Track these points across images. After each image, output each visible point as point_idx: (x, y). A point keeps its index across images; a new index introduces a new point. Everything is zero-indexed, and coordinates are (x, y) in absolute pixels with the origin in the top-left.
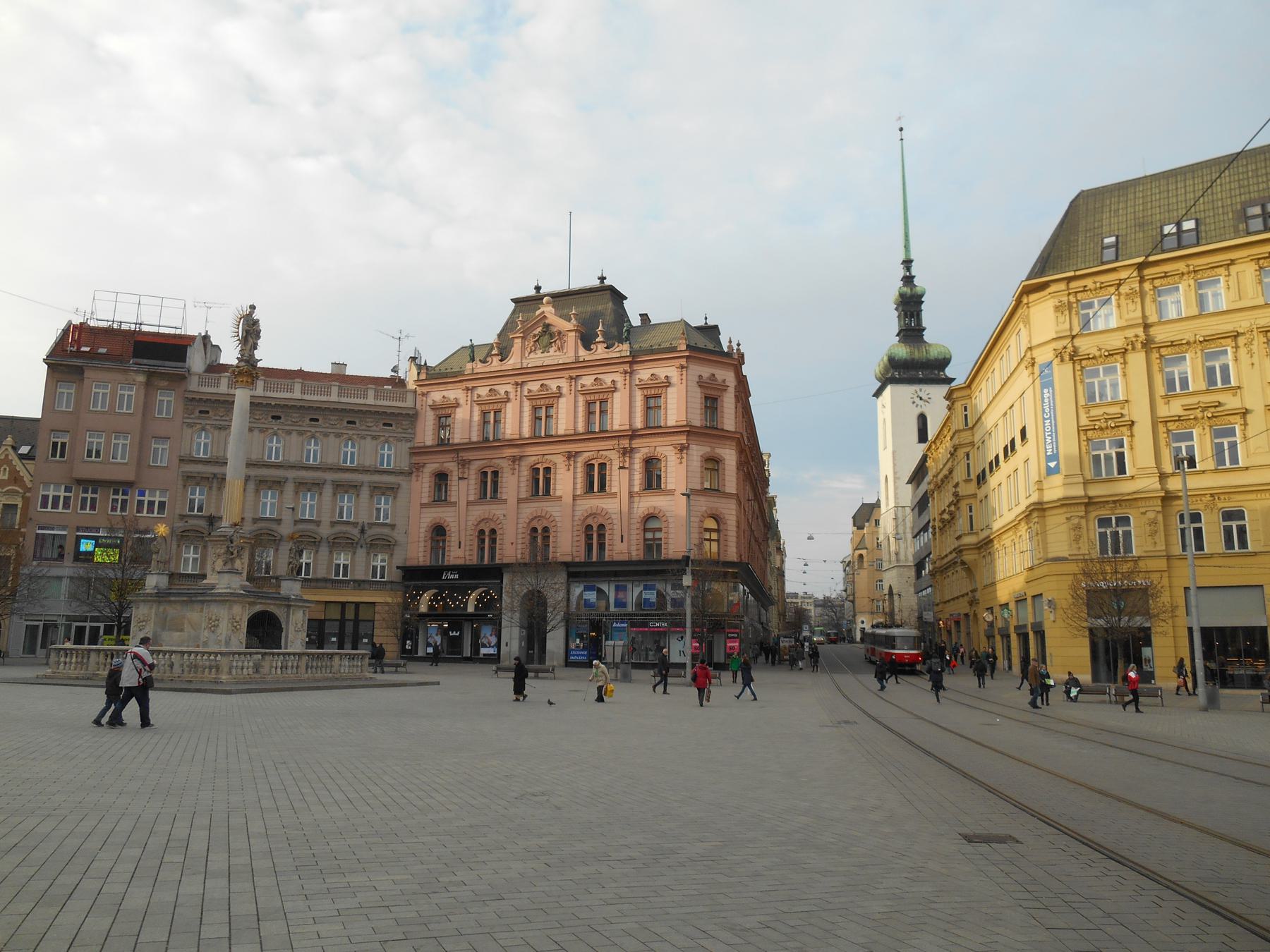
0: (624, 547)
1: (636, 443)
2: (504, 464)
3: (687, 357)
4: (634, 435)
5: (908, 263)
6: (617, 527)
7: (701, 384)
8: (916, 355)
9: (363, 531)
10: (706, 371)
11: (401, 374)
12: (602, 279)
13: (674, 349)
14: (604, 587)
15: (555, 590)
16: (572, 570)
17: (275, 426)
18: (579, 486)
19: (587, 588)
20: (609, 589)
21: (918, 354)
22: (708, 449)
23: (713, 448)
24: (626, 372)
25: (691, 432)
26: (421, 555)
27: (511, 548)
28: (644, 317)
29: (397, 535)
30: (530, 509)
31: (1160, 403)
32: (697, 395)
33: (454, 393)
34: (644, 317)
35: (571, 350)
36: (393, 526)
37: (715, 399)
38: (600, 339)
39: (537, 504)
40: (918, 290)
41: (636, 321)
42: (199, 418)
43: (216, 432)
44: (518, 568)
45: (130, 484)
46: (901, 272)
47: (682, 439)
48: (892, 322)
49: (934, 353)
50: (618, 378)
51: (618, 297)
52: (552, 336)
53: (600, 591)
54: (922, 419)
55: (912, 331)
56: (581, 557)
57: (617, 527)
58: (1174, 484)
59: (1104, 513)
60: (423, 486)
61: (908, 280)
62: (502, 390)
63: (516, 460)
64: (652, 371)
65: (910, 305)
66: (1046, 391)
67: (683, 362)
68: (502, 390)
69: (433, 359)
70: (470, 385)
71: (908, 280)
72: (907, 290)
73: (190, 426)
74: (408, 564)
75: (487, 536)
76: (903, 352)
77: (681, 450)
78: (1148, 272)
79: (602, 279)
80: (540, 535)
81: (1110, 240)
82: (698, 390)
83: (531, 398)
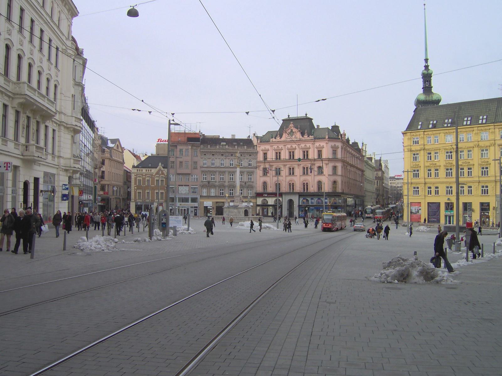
0: (313, 188)
1: (315, 162)
2: (282, 166)
3: (328, 141)
4: (315, 160)
5: (426, 60)
6: (311, 182)
7: (332, 147)
8: (428, 99)
9: (245, 184)
10: (333, 144)
11: (251, 138)
12: (306, 114)
13: (325, 138)
14: (307, 198)
15: (295, 199)
16: (300, 194)
17: (222, 157)
18: (301, 173)
19: (304, 199)
20: (309, 199)
21: (429, 98)
22: (334, 164)
23: (335, 164)
24: (312, 144)
25: (329, 160)
26: (261, 189)
27: (284, 188)
28: (318, 126)
29: (254, 184)
30: (289, 178)
31: (426, 163)
33: (267, 147)
34: (318, 126)
35: (298, 135)
36: (253, 182)
37: (336, 151)
38: (306, 134)
39: (291, 177)
40: (430, 72)
41: (316, 127)
42: (204, 156)
43: (208, 160)
44: (286, 193)
45: (189, 174)
46: (424, 64)
47: (327, 162)
48: (420, 83)
49: (435, 98)
50: (311, 145)
51: (310, 120)
52: (293, 133)
53: (307, 199)
55: (427, 89)
56: (302, 191)
57: (311, 182)
58: (427, 181)
59: (415, 186)
60: (260, 172)
61: (427, 67)
62: (280, 147)
63: (285, 166)
64: (320, 144)
65: (427, 77)
67: (327, 142)
68: (280, 147)
69: (260, 134)
70: (272, 145)
71: (427, 67)
72: (426, 72)
73: (202, 158)
74: (257, 192)
75: (278, 185)
76: (423, 98)
77: (327, 165)
78: (425, 133)
79: (306, 114)
80: (292, 185)
81: (420, 123)
82: (331, 149)
83: (288, 149)
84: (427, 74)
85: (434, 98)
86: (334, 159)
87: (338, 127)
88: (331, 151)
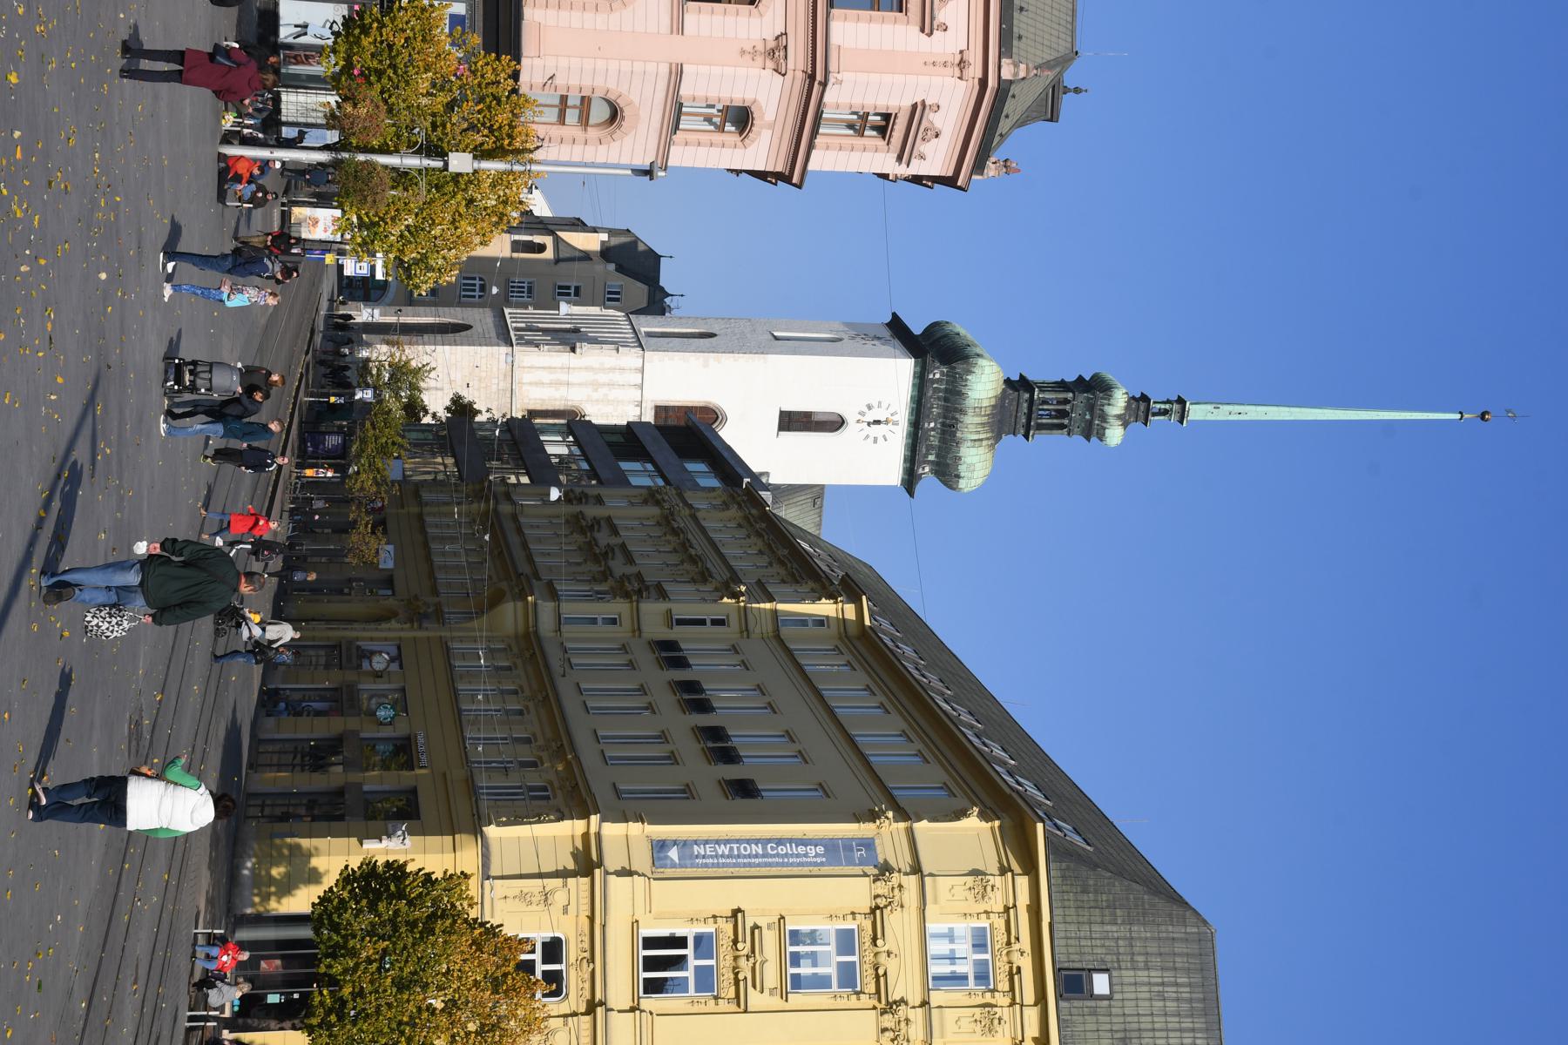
7: (917, 111)
13: (1006, 48)
21: (972, 425)
23: (772, 126)
25: (815, 80)
32: (897, 101)
54: (834, 424)
59: (572, 952)
66: (820, 849)
67: (975, 71)
72: (1119, 402)
82: (907, 104)
84: (1104, 418)
85: (973, 451)
86: (808, 122)
87: (1053, 118)
88: (894, 97)
